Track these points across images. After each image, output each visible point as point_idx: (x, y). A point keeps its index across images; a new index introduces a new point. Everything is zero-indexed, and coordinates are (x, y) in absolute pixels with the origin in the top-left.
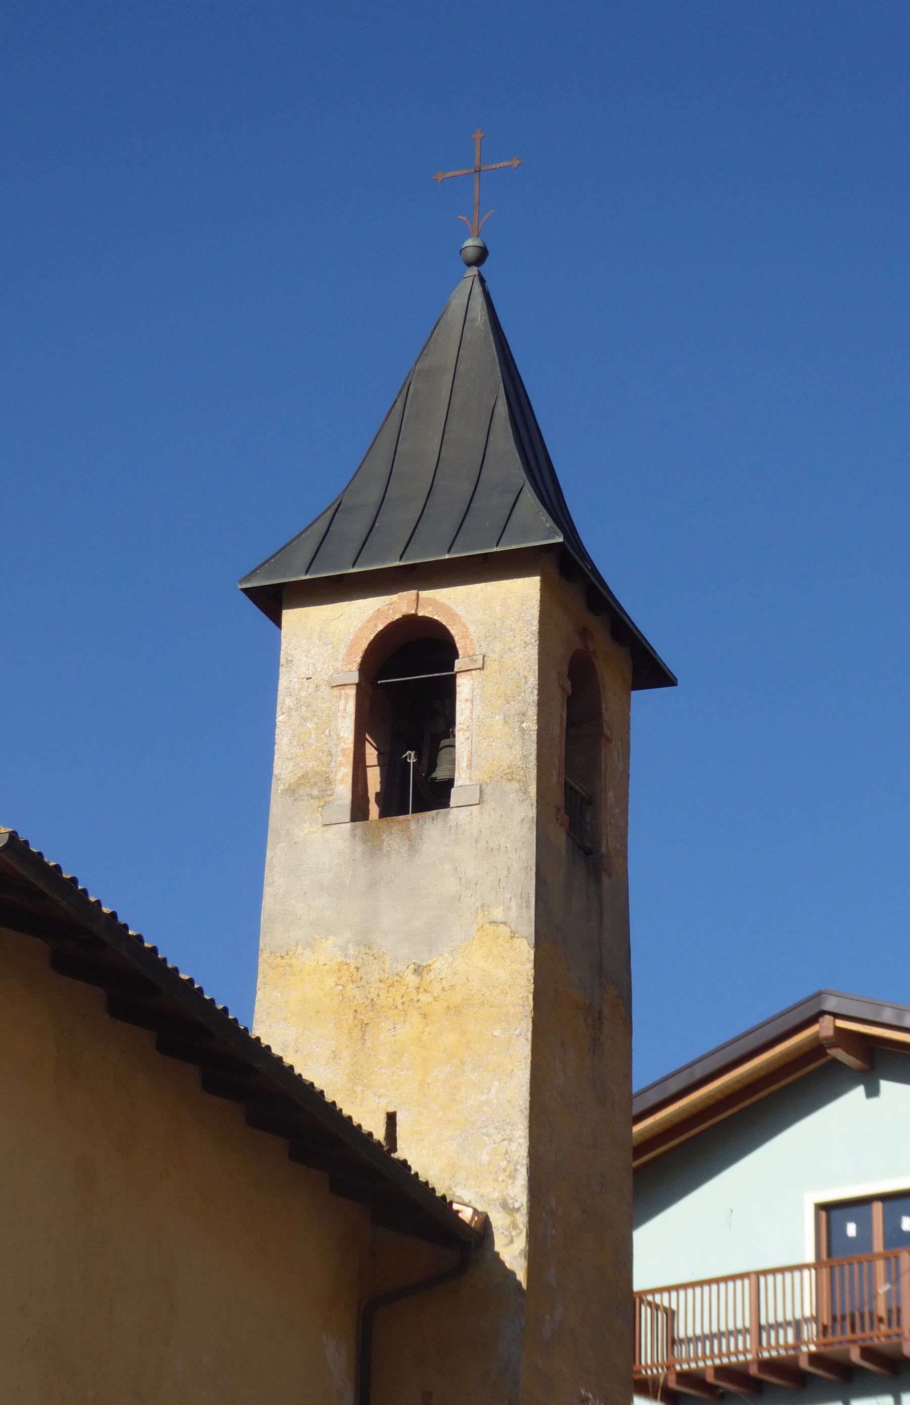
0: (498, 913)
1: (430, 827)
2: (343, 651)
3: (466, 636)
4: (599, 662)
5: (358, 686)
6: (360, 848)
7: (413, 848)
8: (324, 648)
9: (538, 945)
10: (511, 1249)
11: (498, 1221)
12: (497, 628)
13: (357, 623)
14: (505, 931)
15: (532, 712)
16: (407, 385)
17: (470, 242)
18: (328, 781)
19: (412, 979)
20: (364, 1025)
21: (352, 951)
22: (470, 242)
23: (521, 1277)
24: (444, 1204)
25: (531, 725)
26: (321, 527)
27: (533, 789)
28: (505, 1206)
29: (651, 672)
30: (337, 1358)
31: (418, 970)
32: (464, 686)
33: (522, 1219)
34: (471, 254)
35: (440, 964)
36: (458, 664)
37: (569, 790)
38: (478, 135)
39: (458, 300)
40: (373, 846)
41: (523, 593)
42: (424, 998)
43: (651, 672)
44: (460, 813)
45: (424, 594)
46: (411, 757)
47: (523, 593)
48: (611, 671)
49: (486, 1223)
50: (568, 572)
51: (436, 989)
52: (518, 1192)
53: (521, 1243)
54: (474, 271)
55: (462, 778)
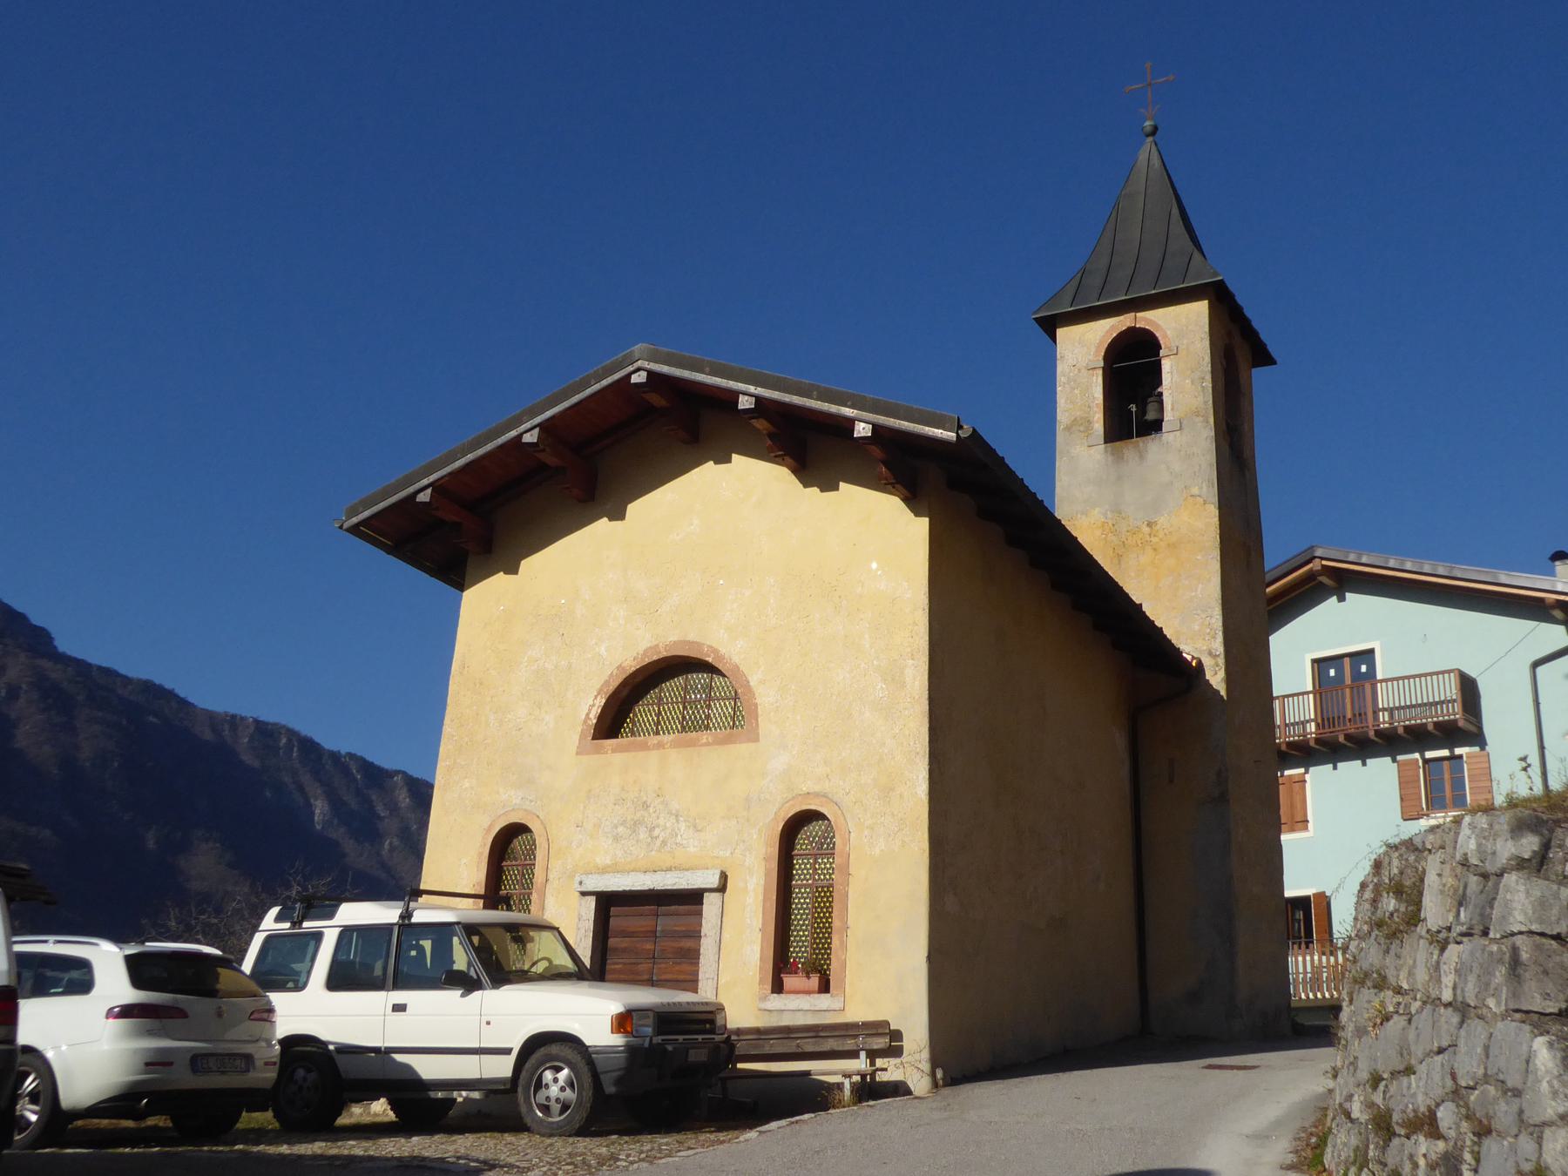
0: (1195, 491)
1: (1152, 447)
2: (1093, 350)
3: (1165, 336)
4: (1239, 349)
5: (1104, 369)
6: (1110, 458)
7: (1142, 457)
8: (1082, 349)
9: (1220, 508)
10: (1216, 678)
11: (1207, 662)
12: (1183, 330)
13: (1101, 334)
14: (1201, 500)
15: (1209, 377)
16: (1117, 204)
17: (1148, 123)
18: (1089, 422)
19: (1146, 530)
20: (1119, 556)
21: (1109, 515)
22: (1148, 123)
23: (1223, 693)
24: (1178, 652)
25: (1208, 384)
26: (1075, 283)
27: (1212, 420)
28: (1210, 654)
29: (1262, 357)
30: (1120, 741)
31: (1149, 525)
32: (1166, 365)
33: (1221, 661)
34: (1148, 129)
35: (1162, 521)
36: (1162, 353)
37: (1228, 425)
38: (1148, 65)
39: (1143, 156)
40: (1119, 457)
41: (1198, 311)
42: (1154, 540)
43: (1262, 357)
44: (1168, 436)
45: (1139, 315)
46: (1133, 408)
47: (1198, 311)
48: (1243, 354)
49: (1200, 663)
50: (1221, 299)
51: (1161, 535)
52: (1218, 645)
53: (1222, 674)
54: (1150, 139)
55: (1168, 415)
